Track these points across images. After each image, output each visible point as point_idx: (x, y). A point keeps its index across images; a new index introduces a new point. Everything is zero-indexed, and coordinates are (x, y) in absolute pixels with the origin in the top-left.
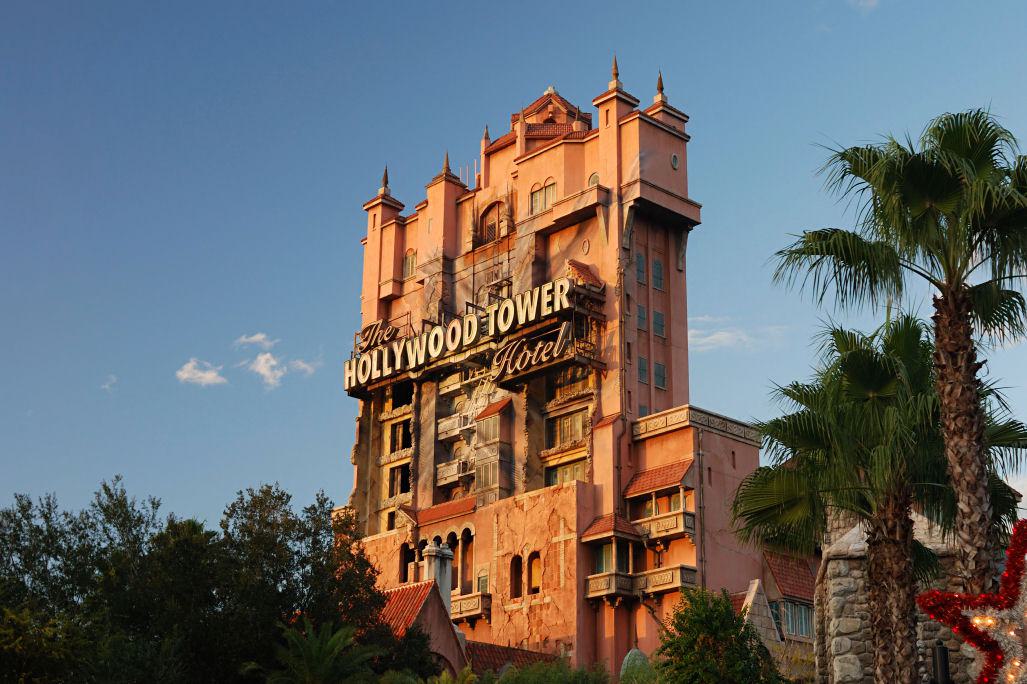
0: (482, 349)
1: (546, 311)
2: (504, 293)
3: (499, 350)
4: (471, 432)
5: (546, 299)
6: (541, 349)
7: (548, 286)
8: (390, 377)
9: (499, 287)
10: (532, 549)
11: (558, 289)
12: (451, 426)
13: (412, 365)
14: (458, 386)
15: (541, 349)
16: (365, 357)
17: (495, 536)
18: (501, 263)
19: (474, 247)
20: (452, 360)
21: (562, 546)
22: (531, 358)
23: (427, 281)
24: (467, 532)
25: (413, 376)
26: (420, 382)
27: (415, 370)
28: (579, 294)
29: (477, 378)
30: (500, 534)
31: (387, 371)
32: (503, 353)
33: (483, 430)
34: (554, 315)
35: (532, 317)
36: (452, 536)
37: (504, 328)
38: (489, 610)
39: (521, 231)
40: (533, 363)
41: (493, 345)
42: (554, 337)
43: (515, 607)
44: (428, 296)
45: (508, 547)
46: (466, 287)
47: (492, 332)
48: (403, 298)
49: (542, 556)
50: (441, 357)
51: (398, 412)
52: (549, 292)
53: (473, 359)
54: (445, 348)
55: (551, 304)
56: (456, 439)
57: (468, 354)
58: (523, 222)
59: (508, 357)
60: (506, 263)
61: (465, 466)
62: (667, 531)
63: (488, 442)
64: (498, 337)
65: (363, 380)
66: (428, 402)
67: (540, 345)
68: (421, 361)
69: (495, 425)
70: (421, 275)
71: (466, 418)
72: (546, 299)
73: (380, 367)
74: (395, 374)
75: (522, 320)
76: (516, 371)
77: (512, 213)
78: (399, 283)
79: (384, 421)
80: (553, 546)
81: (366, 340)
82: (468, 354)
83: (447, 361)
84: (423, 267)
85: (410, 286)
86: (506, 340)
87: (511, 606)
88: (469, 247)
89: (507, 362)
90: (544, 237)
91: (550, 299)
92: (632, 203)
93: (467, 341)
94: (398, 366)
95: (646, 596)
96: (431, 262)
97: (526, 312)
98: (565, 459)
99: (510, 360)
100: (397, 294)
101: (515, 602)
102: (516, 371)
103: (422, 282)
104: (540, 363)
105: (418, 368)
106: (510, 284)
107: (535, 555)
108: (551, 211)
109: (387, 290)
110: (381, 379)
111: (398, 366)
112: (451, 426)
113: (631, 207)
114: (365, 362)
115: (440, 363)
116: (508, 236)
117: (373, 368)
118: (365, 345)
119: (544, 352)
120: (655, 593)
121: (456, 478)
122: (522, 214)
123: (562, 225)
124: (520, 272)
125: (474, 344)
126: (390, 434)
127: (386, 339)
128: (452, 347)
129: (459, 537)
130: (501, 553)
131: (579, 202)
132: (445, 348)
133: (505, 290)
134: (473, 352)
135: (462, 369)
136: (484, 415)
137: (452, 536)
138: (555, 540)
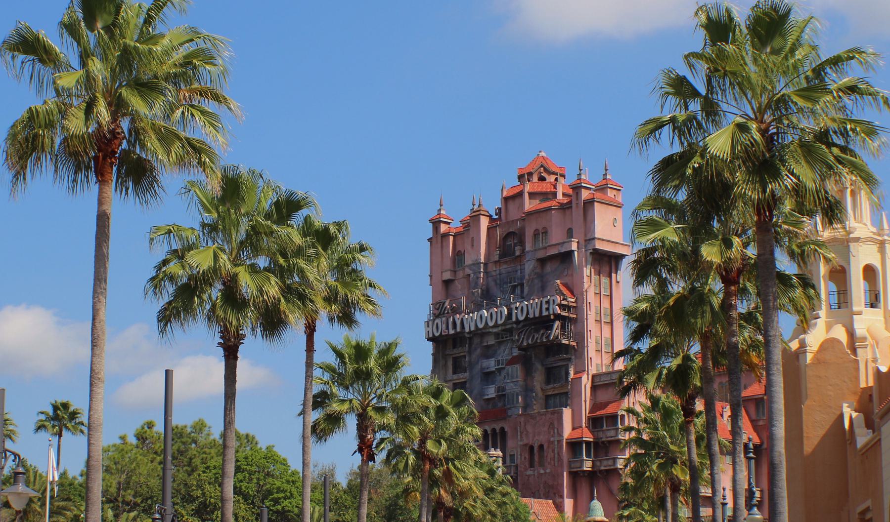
0: (508, 327)
1: (545, 313)
2: (518, 291)
3: (520, 329)
4: (503, 368)
5: (545, 306)
6: (543, 334)
7: (545, 300)
8: (453, 335)
9: (514, 287)
10: (539, 443)
11: (551, 302)
12: (491, 364)
13: (467, 330)
14: (493, 342)
15: (543, 334)
16: (438, 321)
17: (519, 434)
18: (517, 271)
19: (500, 258)
20: (491, 330)
21: (556, 443)
22: (537, 338)
23: (472, 275)
24: (502, 429)
25: (467, 336)
26: (470, 339)
27: (468, 333)
28: (563, 305)
29: (505, 339)
30: (521, 433)
31: (452, 332)
32: (521, 332)
33: (510, 370)
34: (549, 316)
35: (537, 315)
36: (494, 430)
37: (521, 318)
38: (517, 473)
39: (528, 257)
40: (539, 341)
41: (515, 326)
42: (550, 328)
43: (531, 473)
44: (473, 285)
45: (525, 441)
46: (495, 281)
47: (514, 319)
48: (456, 281)
49: (545, 447)
50: (484, 328)
51: (455, 351)
52: (548, 302)
53: (504, 330)
54: (486, 323)
55: (548, 309)
56: (493, 372)
57: (500, 328)
58: (529, 251)
59: (524, 334)
60: (519, 272)
61: (499, 389)
62: (611, 437)
63: (514, 380)
64: (518, 322)
65: (437, 334)
66: (476, 349)
67: (542, 332)
68: (473, 329)
69: (517, 371)
70: (468, 271)
71: (498, 361)
72: (545, 306)
73: (447, 328)
74: (457, 334)
75: (531, 316)
76: (528, 344)
77: (522, 243)
78: (454, 272)
79: (448, 355)
80: (550, 443)
81: (438, 309)
82: (500, 328)
83: (488, 330)
84: (469, 266)
85: (460, 274)
86: (521, 324)
87: (529, 472)
88: (497, 258)
89: (523, 338)
90: (542, 261)
91: (547, 306)
92: (591, 251)
93: (500, 322)
94: (458, 329)
95: (601, 471)
96: (474, 264)
97: (534, 313)
98: (556, 392)
99: (525, 337)
100: (453, 278)
101: (531, 470)
102: (528, 344)
103: (469, 275)
104: (542, 342)
105: (470, 332)
106: (522, 285)
107: (541, 447)
108: (545, 248)
109: (447, 276)
110: (448, 335)
111: (458, 329)
112: (491, 364)
113: (591, 253)
114: (437, 323)
115: (484, 331)
116: (519, 256)
117: (442, 328)
118: (437, 312)
119: (545, 336)
120: (606, 471)
121: (493, 396)
122: (528, 247)
123: (552, 258)
124: (528, 282)
125: (504, 324)
126: (451, 363)
127: (450, 312)
128: (491, 324)
129: (498, 431)
130: (521, 443)
131: (562, 247)
132: (486, 323)
133: (519, 288)
134: (503, 328)
135: (497, 335)
136: (511, 362)
137: (494, 430)
138: (552, 439)
